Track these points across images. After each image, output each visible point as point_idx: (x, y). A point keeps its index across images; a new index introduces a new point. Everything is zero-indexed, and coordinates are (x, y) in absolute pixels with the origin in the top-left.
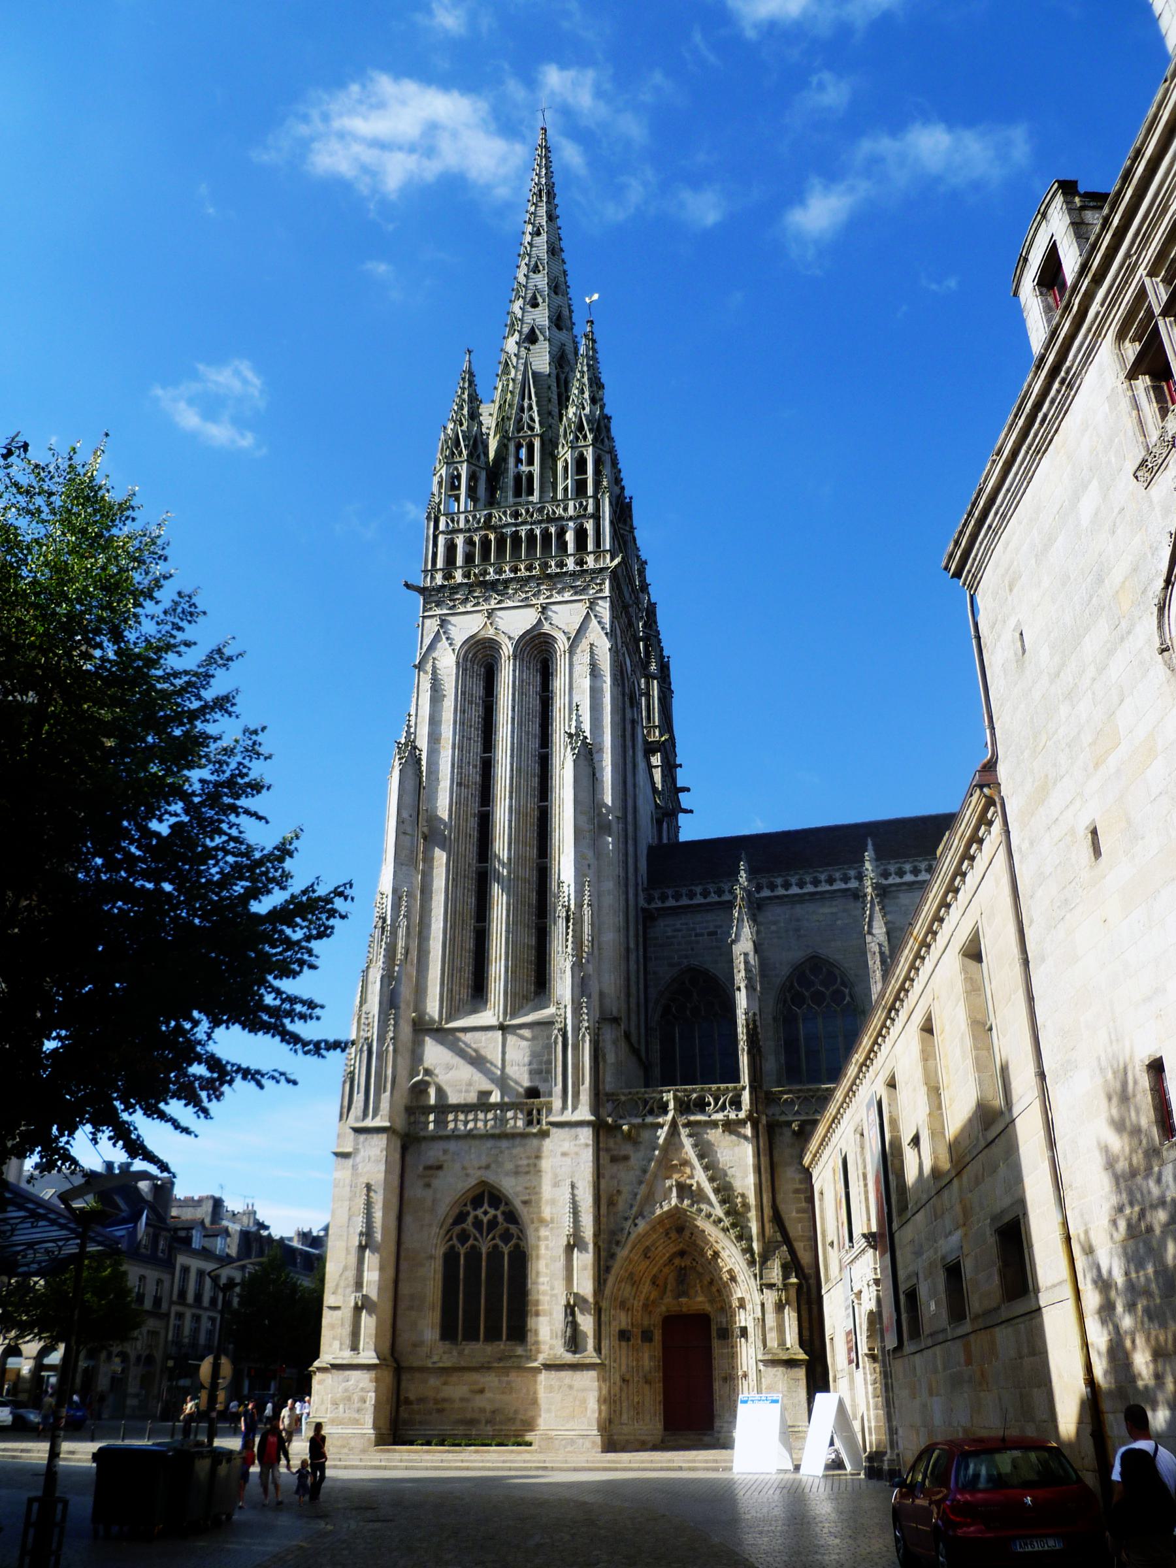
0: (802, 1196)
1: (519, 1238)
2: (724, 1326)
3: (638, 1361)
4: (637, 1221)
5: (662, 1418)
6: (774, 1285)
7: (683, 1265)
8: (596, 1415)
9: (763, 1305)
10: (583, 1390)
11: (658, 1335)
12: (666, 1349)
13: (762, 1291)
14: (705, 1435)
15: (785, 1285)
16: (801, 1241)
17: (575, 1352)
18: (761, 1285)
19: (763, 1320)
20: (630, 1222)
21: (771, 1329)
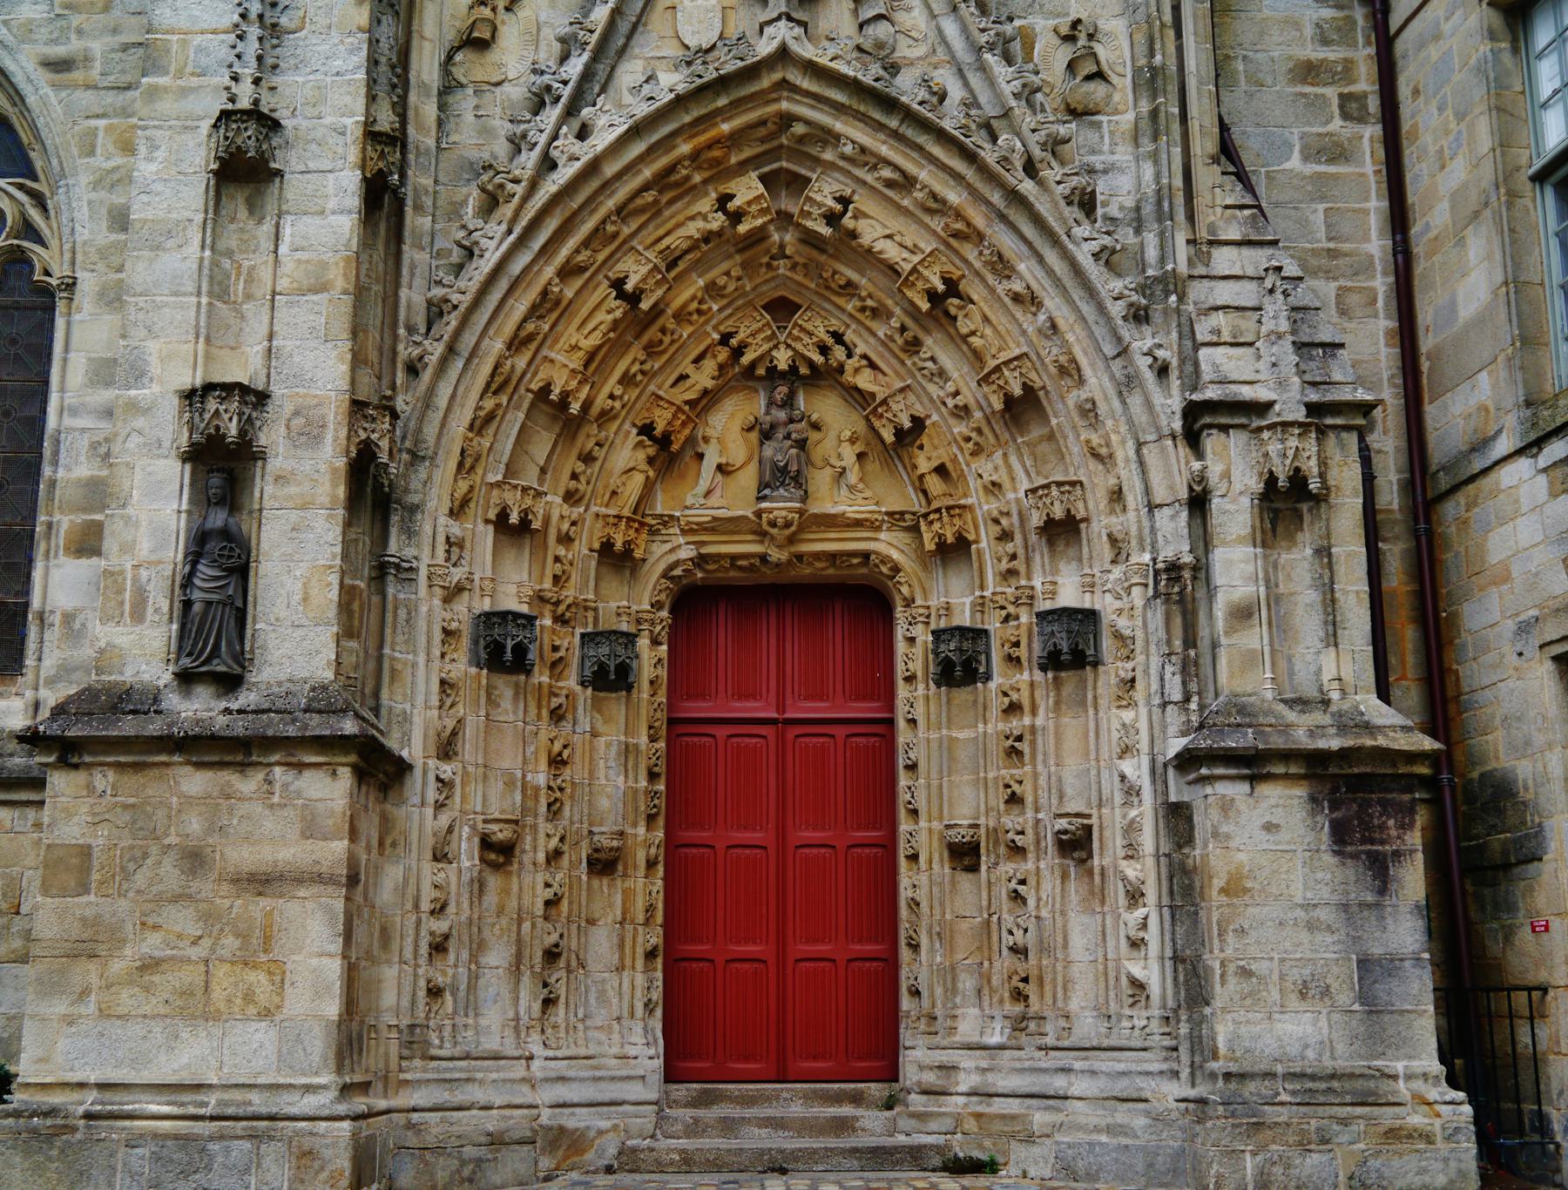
0: (1331, 93)
1: (29, 230)
2: (964, 619)
3: (557, 762)
4: (586, 112)
5: (657, 1024)
6: (1263, 408)
7: (782, 359)
8: (333, 1009)
9: (1198, 503)
10: (261, 882)
11: (650, 659)
12: (677, 726)
13: (1193, 438)
14: (857, 1099)
15: (1313, 409)
16: (1329, 275)
17: (230, 683)
18: (1193, 412)
19: (1201, 569)
20: (552, 114)
21: (1243, 614)
